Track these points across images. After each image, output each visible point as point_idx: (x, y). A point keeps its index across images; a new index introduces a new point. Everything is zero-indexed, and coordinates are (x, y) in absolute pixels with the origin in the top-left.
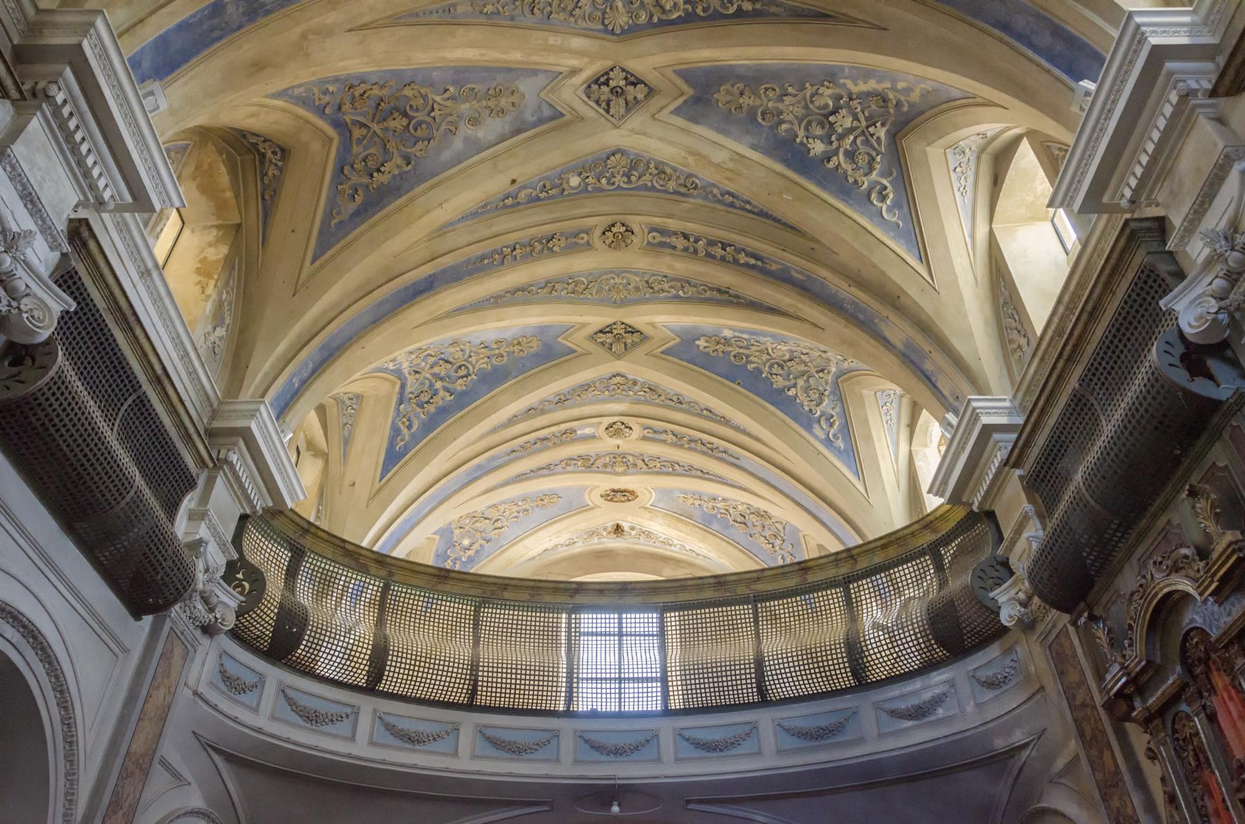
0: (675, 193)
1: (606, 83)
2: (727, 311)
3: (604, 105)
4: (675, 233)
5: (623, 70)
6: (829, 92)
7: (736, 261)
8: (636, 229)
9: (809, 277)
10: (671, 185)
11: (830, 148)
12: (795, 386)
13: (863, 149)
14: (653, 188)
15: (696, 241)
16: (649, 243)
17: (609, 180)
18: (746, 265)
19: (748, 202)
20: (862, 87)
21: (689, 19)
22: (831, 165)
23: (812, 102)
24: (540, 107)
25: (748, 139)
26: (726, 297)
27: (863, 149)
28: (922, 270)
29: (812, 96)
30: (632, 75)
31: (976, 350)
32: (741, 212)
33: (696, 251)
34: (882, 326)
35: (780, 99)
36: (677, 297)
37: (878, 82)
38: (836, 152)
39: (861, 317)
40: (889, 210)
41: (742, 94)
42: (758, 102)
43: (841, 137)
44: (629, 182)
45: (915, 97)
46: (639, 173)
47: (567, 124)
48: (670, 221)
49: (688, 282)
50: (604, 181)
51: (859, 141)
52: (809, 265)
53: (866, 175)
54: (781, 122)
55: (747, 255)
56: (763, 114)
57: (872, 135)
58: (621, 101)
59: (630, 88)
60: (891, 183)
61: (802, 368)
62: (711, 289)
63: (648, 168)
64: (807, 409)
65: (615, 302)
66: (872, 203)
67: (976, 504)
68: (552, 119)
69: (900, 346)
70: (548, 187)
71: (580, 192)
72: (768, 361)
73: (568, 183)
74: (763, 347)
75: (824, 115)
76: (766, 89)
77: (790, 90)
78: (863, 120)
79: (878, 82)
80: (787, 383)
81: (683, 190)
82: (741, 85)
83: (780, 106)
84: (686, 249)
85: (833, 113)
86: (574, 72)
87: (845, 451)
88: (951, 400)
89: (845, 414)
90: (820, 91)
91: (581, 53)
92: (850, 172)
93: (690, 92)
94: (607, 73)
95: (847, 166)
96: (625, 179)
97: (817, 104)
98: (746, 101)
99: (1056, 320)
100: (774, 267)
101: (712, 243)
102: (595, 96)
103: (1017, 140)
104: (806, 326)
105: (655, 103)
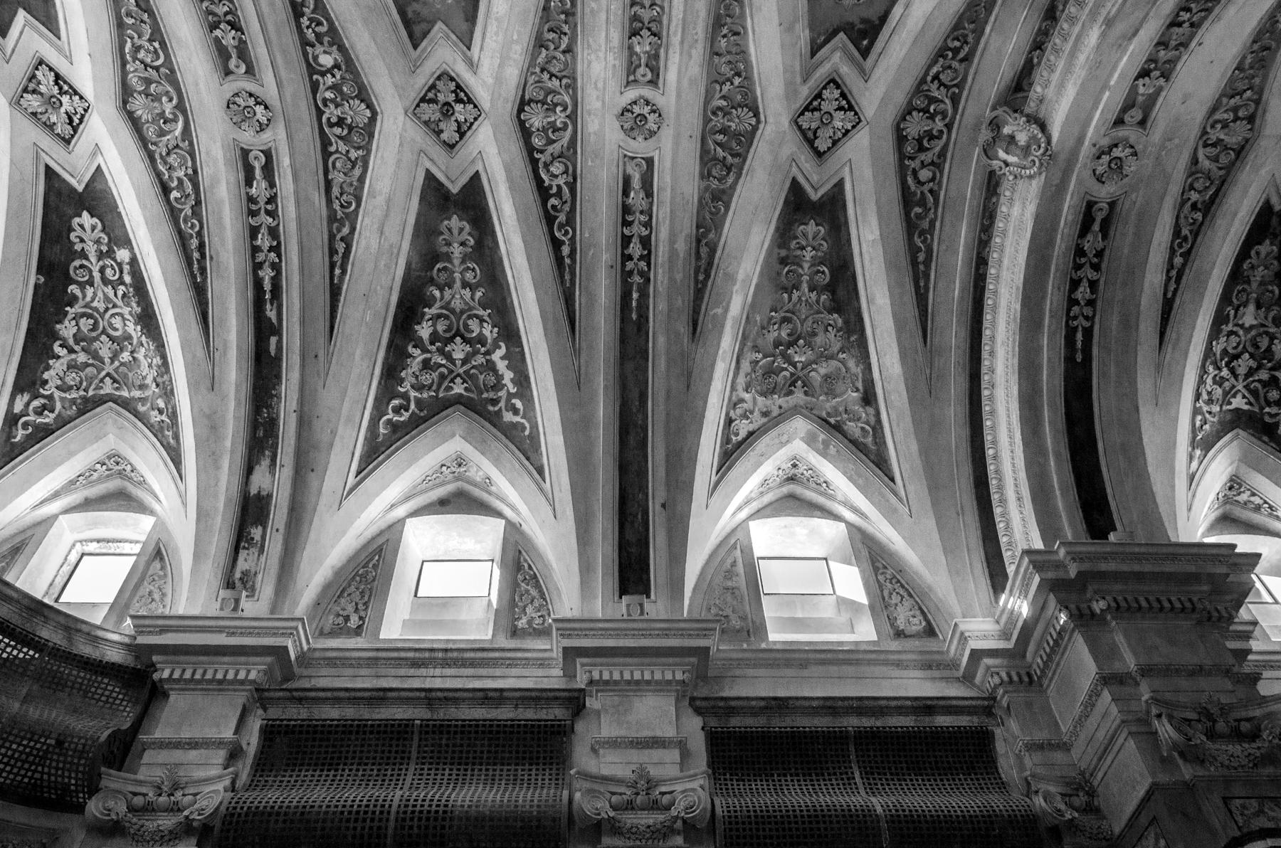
0: (328, 184)
1: (458, 101)
2: (175, 262)
3: (430, 95)
4: (272, 185)
5: (476, 119)
6: (487, 332)
7: (257, 266)
8: (267, 136)
9: (278, 358)
10: (337, 177)
11: (427, 342)
12: (71, 351)
13: (435, 375)
14: (326, 154)
15: (268, 213)
16: (245, 153)
17: (332, 101)
18: (258, 284)
19: (344, 272)
20: (501, 366)
21: (543, 192)
22: (410, 349)
23: (470, 317)
24: (424, 20)
25: (416, 259)
26: (196, 255)
27: (435, 375)
28: (351, 480)
29: (477, 316)
30: (469, 128)
31: (311, 576)
32: (327, 264)
33: (253, 214)
34: (265, 463)
35: (465, 285)
36: (166, 190)
37: (512, 380)
38: (425, 350)
39: (261, 433)
40: (389, 421)
41: (463, 244)
42: (456, 262)
43: (441, 351)
44: (331, 125)
45: (508, 417)
46: (342, 135)
47: (405, 54)
48: (290, 178)
49: (198, 202)
50: (329, 95)
51: (442, 369)
52: (296, 359)
53: (412, 387)
54: (441, 290)
55: (273, 278)
56: (445, 269)
57: (452, 381)
58: (438, 115)
59: (454, 126)
60: (413, 413)
61: (105, 353)
62: (200, 234)
63: (358, 148)
64: (46, 376)
65: (125, 102)
66: (388, 404)
67: (166, 674)
68: (411, 36)
69: (253, 491)
70: (318, 29)
71: (308, 64)
72: (96, 309)
73: (325, 52)
74: (119, 303)
75: (458, 329)
76: (473, 270)
77: (479, 294)
78: (465, 368)
79: (512, 380)
80: (71, 342)
81: (335, 191)
82: (472, 242)
83: (458, 284)
84: (251, 200)
85: (465, 340)
86: (472, 65)
87: (12, 444)
88: (238, 575)
89: (62, 423)
90: (485, 325)
91: (499, 79)
92: (410, 371)
93: (455, 189)
94: (470, 101)
95: (415, 365)
96: (334, 120)
97: (470, 322)
98: (457, 251)
99: (427, 655)
100: (271, 314)
101: (273, 232)
102: (440, 85)
103: (499, 514)
104: (205, 367)
105: (437, 152)
